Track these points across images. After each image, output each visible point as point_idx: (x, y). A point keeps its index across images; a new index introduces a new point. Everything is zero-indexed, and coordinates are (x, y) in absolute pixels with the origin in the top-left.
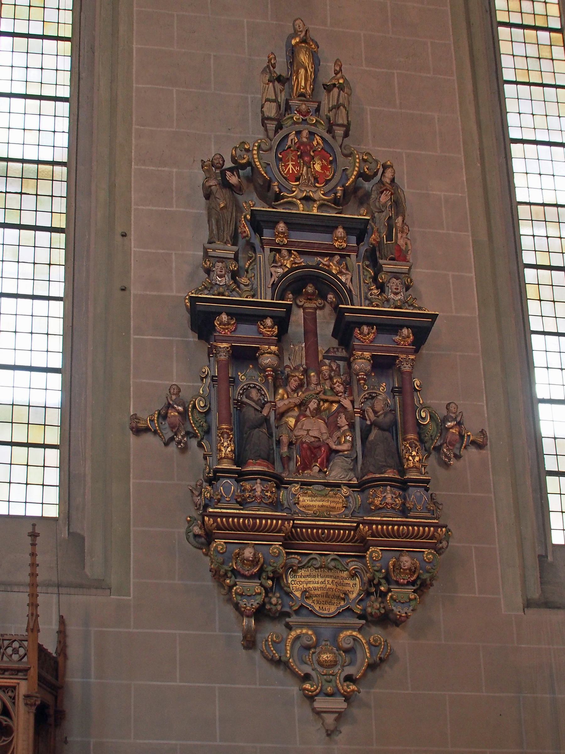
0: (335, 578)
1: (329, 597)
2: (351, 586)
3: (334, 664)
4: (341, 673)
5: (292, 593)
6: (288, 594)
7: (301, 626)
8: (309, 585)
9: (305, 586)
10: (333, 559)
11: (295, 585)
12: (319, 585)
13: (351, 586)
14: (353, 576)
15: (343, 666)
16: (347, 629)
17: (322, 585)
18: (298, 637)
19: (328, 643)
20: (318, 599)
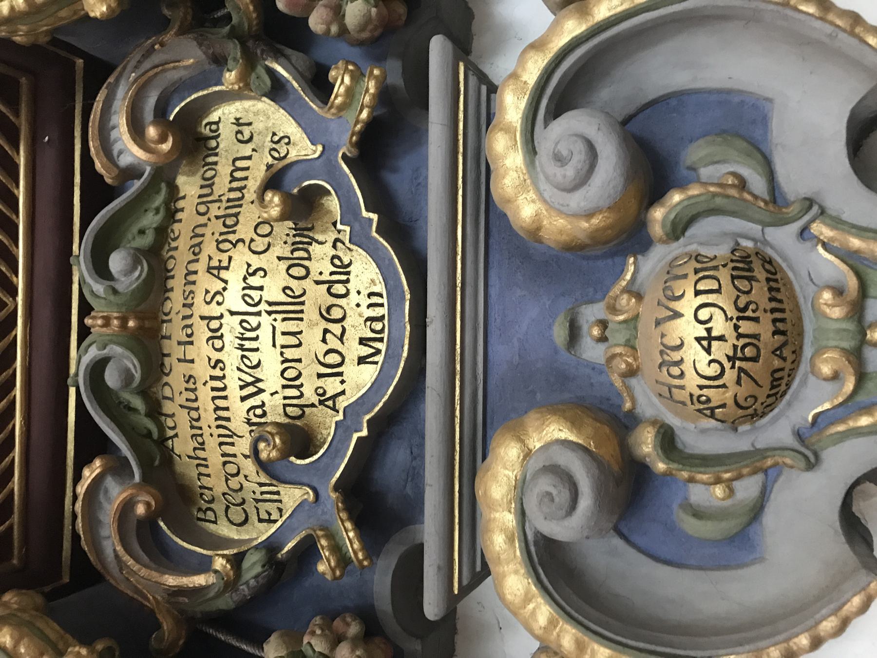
0: (196, 250)
1: (298, 299)
2: (246, 150)
3: (757, 276)
4: (837, 222)
5: (271, 547)
6: (287, 568)
7: (469, 514)
8: (238, 424)
9: (243, 446)
10: (102, 270)
11: (250, 507)
12: (231, 357)
13: (246, 150)
14: (193, 142)
15: (776, 204)
16: (483, 172)
17: (230, 340)
18: (551, 563)
19: (591, 313)
20: (309, 370)
